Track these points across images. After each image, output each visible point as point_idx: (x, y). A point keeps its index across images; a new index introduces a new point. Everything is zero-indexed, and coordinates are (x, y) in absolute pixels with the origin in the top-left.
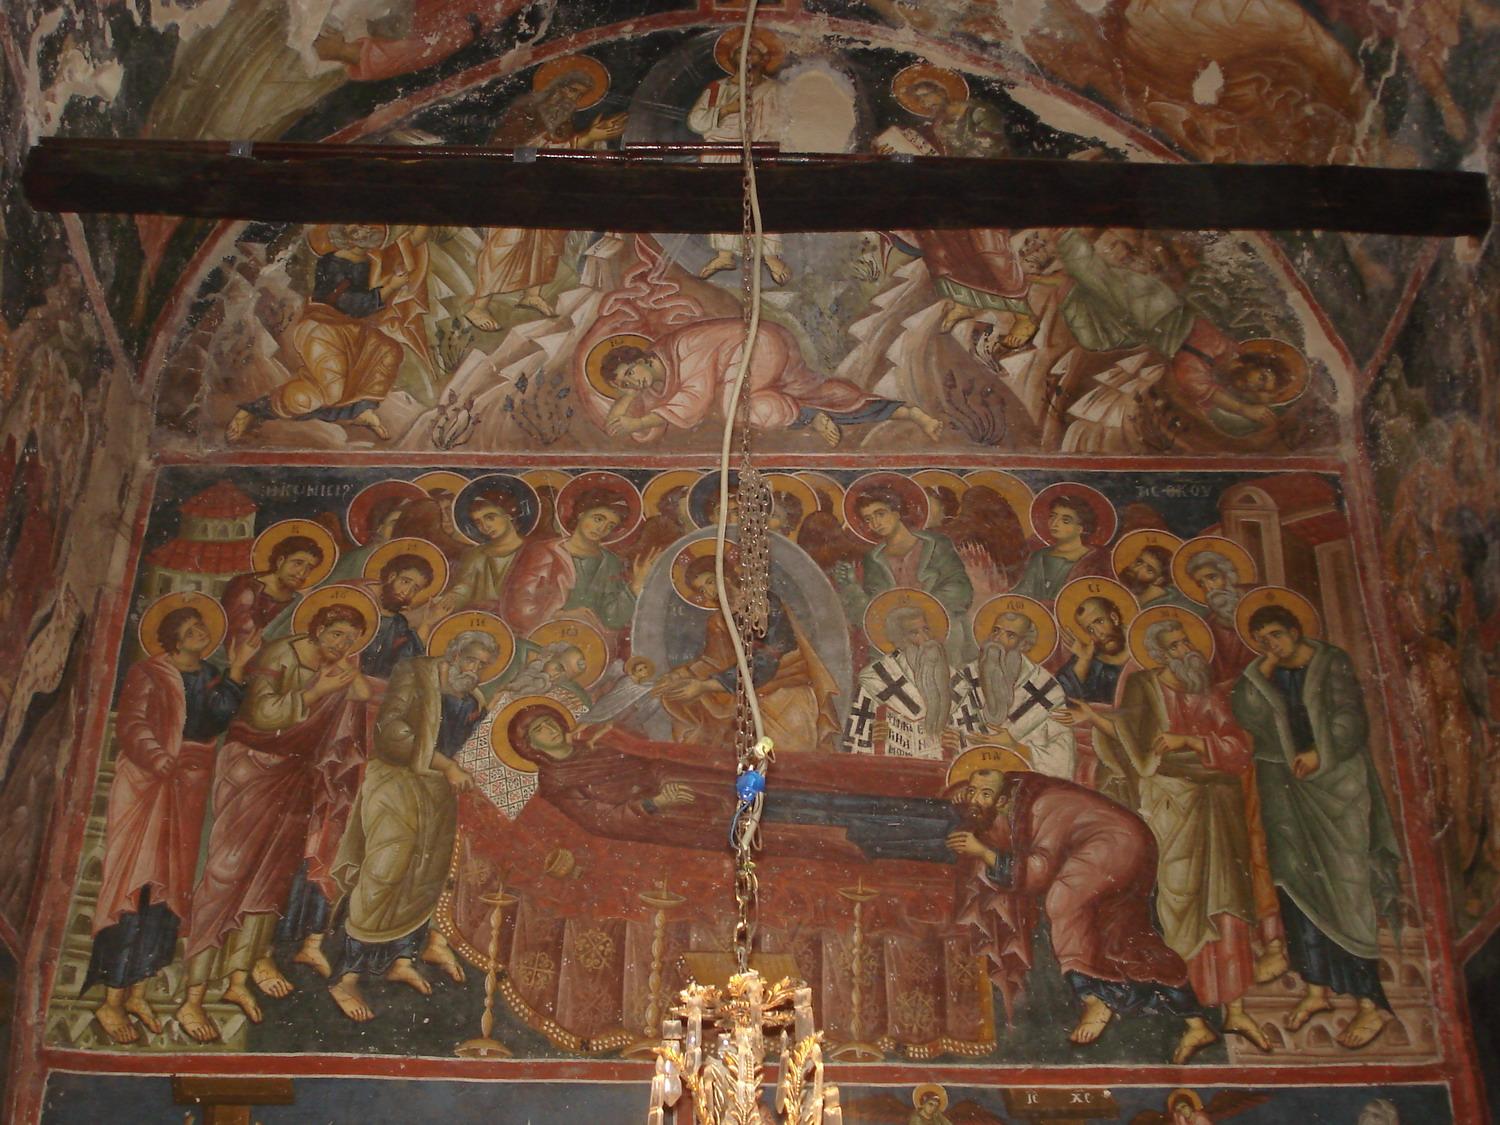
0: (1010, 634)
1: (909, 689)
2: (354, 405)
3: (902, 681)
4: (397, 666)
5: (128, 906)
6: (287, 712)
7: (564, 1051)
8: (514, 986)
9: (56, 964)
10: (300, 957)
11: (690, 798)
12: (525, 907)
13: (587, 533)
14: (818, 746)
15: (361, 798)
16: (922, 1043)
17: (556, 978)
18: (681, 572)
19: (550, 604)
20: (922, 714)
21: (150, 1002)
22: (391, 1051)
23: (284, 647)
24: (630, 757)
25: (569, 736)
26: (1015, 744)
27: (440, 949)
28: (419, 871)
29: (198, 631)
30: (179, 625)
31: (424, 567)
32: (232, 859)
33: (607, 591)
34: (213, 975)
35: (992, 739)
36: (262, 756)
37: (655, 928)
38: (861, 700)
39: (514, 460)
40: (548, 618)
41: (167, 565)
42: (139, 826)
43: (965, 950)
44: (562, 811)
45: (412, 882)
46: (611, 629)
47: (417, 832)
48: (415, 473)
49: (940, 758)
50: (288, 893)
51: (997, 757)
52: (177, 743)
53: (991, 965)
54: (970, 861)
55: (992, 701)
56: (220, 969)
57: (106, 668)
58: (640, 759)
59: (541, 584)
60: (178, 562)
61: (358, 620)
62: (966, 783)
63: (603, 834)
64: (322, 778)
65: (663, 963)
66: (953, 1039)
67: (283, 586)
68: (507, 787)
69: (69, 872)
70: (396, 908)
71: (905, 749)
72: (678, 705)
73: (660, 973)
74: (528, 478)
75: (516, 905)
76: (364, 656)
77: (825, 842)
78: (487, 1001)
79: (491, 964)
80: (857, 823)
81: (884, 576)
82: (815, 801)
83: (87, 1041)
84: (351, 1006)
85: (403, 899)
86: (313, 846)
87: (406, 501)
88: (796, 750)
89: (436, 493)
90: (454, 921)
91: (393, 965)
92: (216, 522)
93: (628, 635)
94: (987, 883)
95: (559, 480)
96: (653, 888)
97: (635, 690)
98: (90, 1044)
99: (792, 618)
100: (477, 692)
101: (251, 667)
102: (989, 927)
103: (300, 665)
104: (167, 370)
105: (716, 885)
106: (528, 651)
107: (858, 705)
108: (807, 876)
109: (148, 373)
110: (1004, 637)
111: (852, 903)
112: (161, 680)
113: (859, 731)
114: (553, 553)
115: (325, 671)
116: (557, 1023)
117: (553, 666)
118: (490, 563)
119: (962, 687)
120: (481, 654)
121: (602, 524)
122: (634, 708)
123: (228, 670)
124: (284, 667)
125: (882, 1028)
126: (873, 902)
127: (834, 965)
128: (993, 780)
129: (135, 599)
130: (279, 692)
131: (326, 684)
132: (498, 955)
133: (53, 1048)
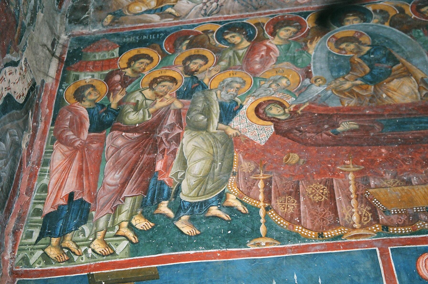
2: (162, 8)
4: (194, 95)
5: (62, 202)
6: (141, 117)
7: (310, 239)
8: (276, 212)
9: (22, 231)
10: (157, 211)
11: (357, 127)
12: (276, 178)
13: (282, 36)
14: (421, 99)
15: (182, 145)
17: (299, 206)
18: (332, 45)
21: (74, 242)
22: (211, 248)
23: (138, 93)
24: (319, 115)
25: (287, 110)
27: (232, 200)
28: (216, 170)
29: (93, 93)
30: (84, 91)
32: (117, 176)
33: (296, 55)
34: (109, 225)
36: (129, 135)
39: (242, 16)
41: (76, 70)
42: (67, 169)
44: (289, 138)
45: (214, 174)
46: (301, 68)
48: (194, 26)
50: (148, 185)
52: (85, 135)
56: (113, 223)
57: (48, 110)
58: (326, 114)
59: (261, 58)
60: (83, 68)
61: (173, 80)
63: (313, 145)
65: (358, 195)
67: (134, 71)
68: (260, 133)
69: (29, 191)
70: (206, 186)
73: (357, 199)
74: (250, 21)
75: (271, 178)
76: (178, 93)
78: (262, 221)
79: (262, 204)
83: (39, 264)
84: (187, 230)
85: (210, 182)
86: (159, 166)
87: (191, 36)
88: (410, 102)
89: (206, 32)
91: (208, 210)
92: (100, 53)
93: (310, 69)
95: (264, 20)
96: (344, 164)
97: (317, 90)
98: (40, 266)
99: (394, 53)
101: (119, 103)
103: (146, 99)
104: (73, 6)
105: (379, 160)
106: (259, 81)
109: (63, 7)
112: (76, 112)
114: (266, 46)
115: (159, 100)
116: (303, 227)
117: (274, 86)
118: (236, 53)
121: (289, 33)
122: (318, 96)
123: (110, 105)
124: (138, 101)
129: (61, 84)
131: (159, 104)
133: (20, 269)
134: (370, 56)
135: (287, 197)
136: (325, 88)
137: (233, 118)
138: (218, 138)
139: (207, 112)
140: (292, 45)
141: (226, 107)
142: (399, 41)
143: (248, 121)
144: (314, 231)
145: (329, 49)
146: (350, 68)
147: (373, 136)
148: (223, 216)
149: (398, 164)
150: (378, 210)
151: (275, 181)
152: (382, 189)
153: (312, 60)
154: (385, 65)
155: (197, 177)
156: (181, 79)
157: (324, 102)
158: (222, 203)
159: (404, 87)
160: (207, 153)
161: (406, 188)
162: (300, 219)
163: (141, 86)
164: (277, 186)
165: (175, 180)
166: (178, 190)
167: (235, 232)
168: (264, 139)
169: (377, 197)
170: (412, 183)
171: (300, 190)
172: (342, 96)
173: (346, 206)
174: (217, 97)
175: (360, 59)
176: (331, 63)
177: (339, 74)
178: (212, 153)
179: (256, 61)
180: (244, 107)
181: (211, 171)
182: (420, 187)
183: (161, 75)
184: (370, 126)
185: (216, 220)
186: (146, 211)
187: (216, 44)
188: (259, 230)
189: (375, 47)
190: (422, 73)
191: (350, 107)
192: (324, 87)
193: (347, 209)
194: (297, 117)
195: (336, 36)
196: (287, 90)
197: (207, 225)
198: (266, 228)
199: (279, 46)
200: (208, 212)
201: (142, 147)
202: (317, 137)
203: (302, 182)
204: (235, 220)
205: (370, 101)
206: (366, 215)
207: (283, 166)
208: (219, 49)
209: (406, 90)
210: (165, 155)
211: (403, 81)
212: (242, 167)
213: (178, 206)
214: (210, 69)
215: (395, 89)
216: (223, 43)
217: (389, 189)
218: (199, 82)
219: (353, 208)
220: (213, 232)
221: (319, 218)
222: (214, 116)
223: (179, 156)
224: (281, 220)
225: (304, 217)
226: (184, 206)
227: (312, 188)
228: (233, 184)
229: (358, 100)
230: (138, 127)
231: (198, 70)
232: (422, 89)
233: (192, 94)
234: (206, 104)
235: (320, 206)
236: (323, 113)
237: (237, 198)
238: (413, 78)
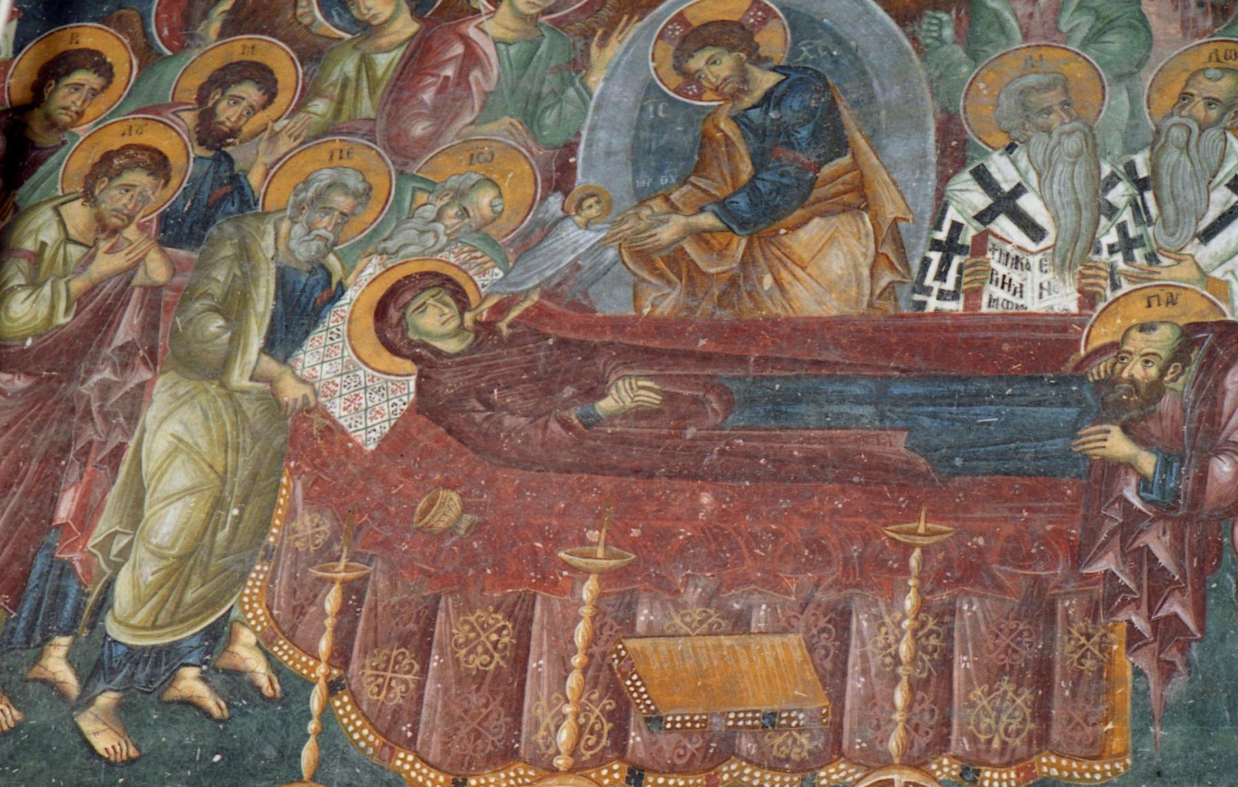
0: (1211, 102)
1: (1030, 204)
3: (1019, 190)
4: (213, 230)
6: (43, 310)
8: (356, 703)
10: (36, 672)
14: (870, 305)
15: (144, 431)
16: (1008, 765)
17: (421, 686)
18: (667, 51)
19: (457, 115)
20: (1048, 241)
24: (563, 343)
25: (468, 317)
26: (1204, 275)
27: (246, 652)
28: (222, 535)
31: (263, 76)
35: (1165, 273)
37: (581, 603)
38: (946, 226)
40: (449, 139)
43: (1092, 613)
44: (449, 432)
47: (223, 480)
49: (1074, 308)
50: (26, 575)
51: (1172, 301)
53: (1134, 637)
54: (1114, 469)
55: (1170, 209)
58: (581, 344)
59: (441, 90)
61: (158, 164)
62: (1115, 346)
63: (509, 463)
64: (89, 401)
65: (591, 656)
66: (1060, 756)
71: (1016, 300)
72: (644, 256)
73: (584, 671)
76: (164, 218)
77: (870, 455)
78: (312, 726)
79: (322, 669)
80: (926, 422)
81: (1003, 29)
82: (856, 390)
84: (105, 741)
86: (66, 508)
88: (834, 313)
90: (269, 608)
91: (173, 677)
93: (574, 154)
94: (1137, 503)
96: (583, 541)
97: (576, 239)
99: (843, 107)
100: (332, 260)
102: (1136, 574)
103: (68, 240)
106: (414, 190)
107: (942, 235)
108: (835, 511)
110: (1199, 109)
111: (909, 548)
113: (941, 276)
114: (465, 39)
115: (104, 245)
118: (366, 63)
119: (1120, 194)
120: (341, 201)
122: (575, 266)
124: (44, 245)
125: (942, 743)
126: (943, 546)
127: (869, 647)
128: (1163, 339)
130: (34, 284)
131: (106, 264)
132: (332, 656)
134: (767, 113)
135: (395, 653)
136: (602, 235)
137: (307, 333)
138: (249, 414)
139: (233, 308)
140: (543, 48)
141: (293, 290)
142: (872, 55)
143: (348, 352)
144: (444, 772)
145: (653, 72)
146: (696, 158)
147: (693, 439)
148: (210, 701)
149: (731, 551)
150: (632, 712)
151: (375, 593)
152: (662, 640)
153: (590, 113)
154: (803, 158)
155: (163, 557)
156: (184, 160)
157: (586, 295)
158: (215, 657)
159: (834, 251)
160: (207, 469)
161: (727, 641)
162: (415, 730)
163: (59, 186)
164: (376, 606)
165: (102, 562)
166: (104, 599)
167: (232, 757)
168: (377, 427)
169: (641, 670)
170: (749, 624)
171: (437, 631)
172: (644, 274)
173: (550, 694)
174: (276, 249)
175: (733, 125)
176: (642, 135)
177: (656, 180)
178: (220, 469)
179: (422, 101)
180: (350, 294)
181: (207, 539)
182: (766, 640)
183: (128, 140)
184: (695, 400)
185: (190, 714)
186: (8, 667)
187: (315, 19)
188: (299, 756)
189: (796, 76)
190: (900, 202)
191: (657, 320)
192: (599, 231)
193: (549, 703)
194: (494, 346)
195: (688, 16)
196: (486, 238)
197: (160, 731)
198: (320, 750)
199: (502, 47)
200: (170, 685)
201: (29, 428)
202: (532, 433)
203: (447, 603)
204: (238, 720)
205: (721, 302)
206: (597, 727)
207: (409, 536)
208: (319, 41)
209: (836, 263)
210: (89, 468)
211: (837, 229)
212: (295, 532)
213: (95, 657)
214: (277, 127)
215: (806, 256)
216: (336, 19)
217: (681, 640)
218: (234, 178)
219: (567, 701)
220: (172, 756)
221: (468, 729)
222: (254, 327)
223: (128, 473)
224: (362, 727)
225: (427, 723)
226: (111, 657)
227: (471, 624)
228: (256, 591)
229: (688, 294)
230: (29, 350)
231: (240, 130)
232: (883, 263)
233: (205, 229)
234: (238, 273)
235: (478, 689)
236: (572, 336)
237: (258, 644)
238: (867, 219)
